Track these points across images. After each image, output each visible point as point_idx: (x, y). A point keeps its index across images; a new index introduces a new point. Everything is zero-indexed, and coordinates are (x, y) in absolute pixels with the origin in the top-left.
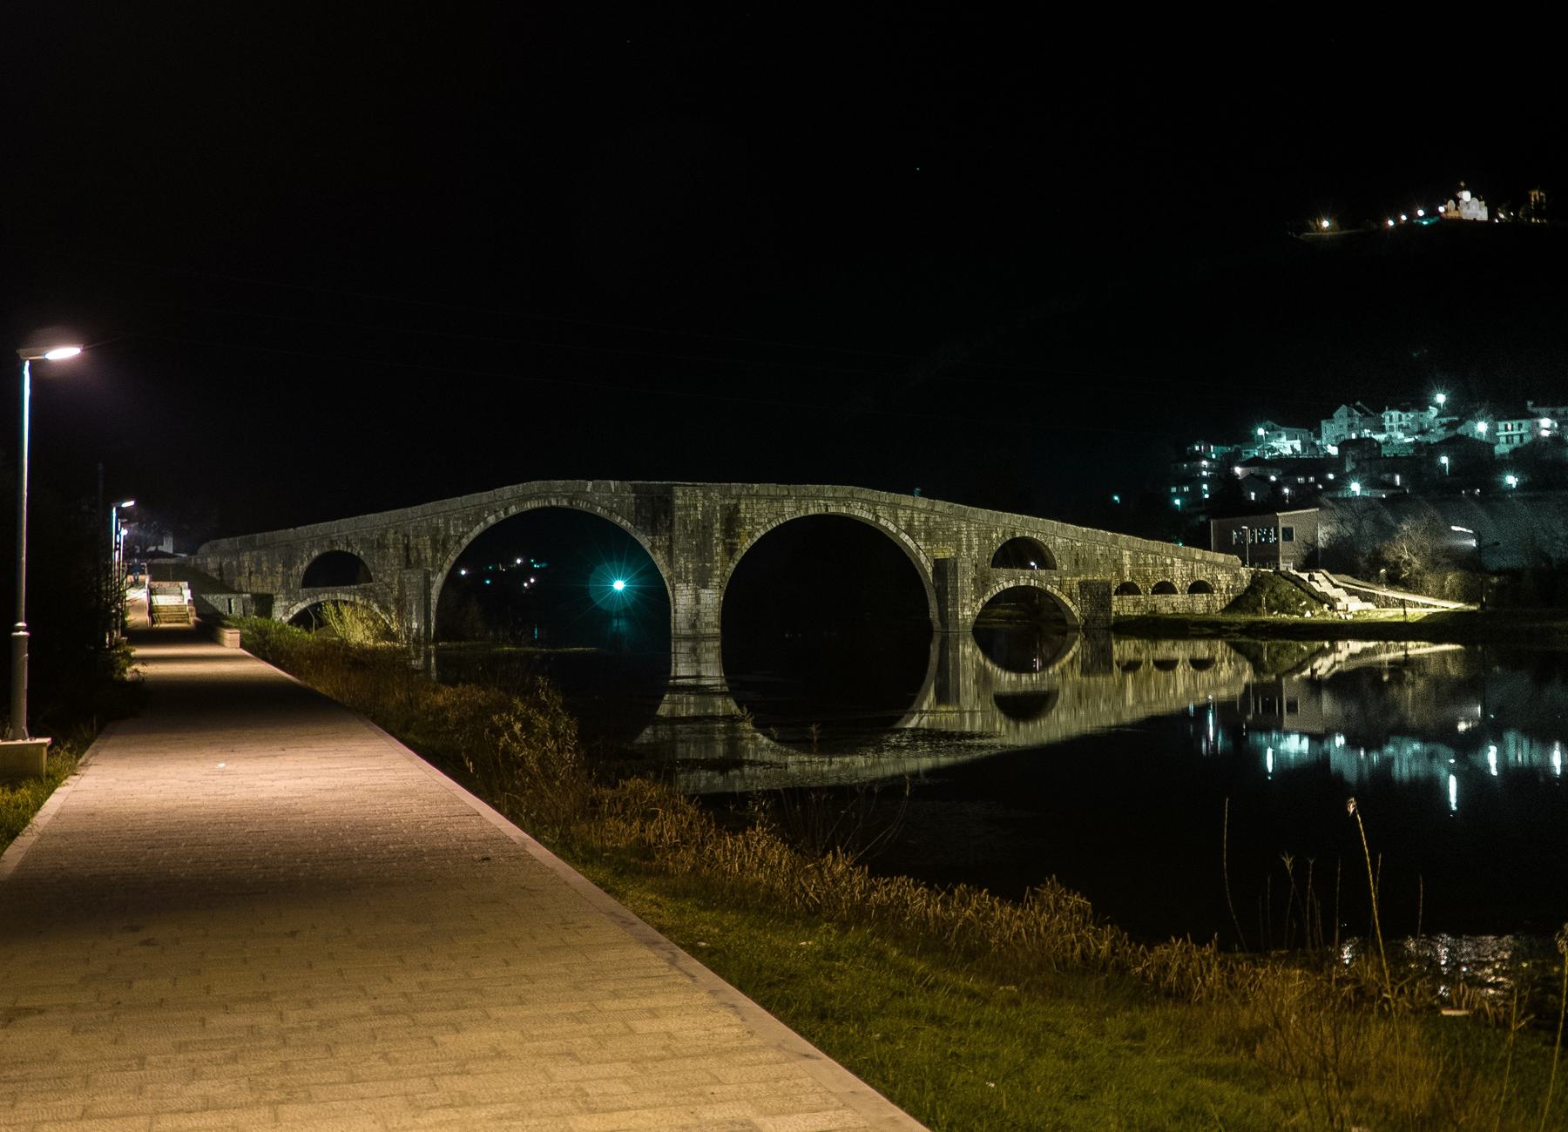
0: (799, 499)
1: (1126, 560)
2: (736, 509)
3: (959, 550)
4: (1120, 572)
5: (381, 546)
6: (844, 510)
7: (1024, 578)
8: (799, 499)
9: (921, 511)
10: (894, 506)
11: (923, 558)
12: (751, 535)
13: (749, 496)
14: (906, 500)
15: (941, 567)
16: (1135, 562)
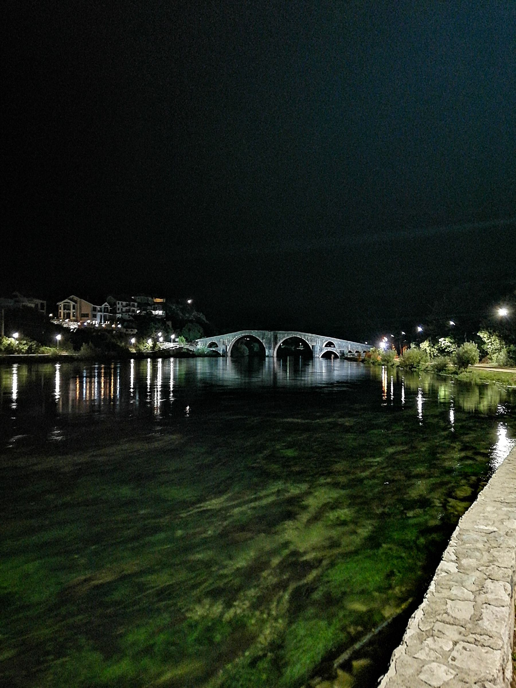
0: (288, 334)
1: (349, 346)
2: (277, 336)
3: (317, 343)
4: (348, 349)
5: (220, 341)
6: (296, 336)
7: (329, 349)
8: (288, 334)
9: (310, 336)
10: (305, 335)
11: (310, 345)
12: (279, 340)
13: (279, 333)
14: (307, 334)
15: (313, 346)
16: (351, 346)
